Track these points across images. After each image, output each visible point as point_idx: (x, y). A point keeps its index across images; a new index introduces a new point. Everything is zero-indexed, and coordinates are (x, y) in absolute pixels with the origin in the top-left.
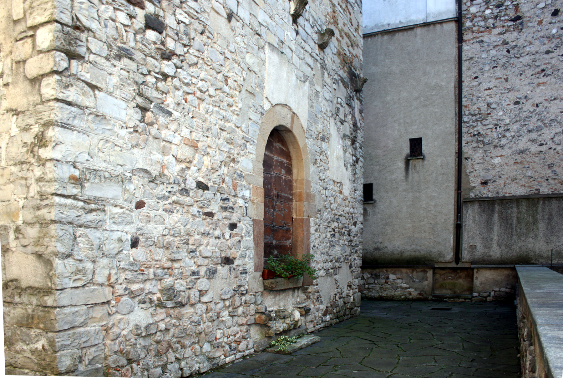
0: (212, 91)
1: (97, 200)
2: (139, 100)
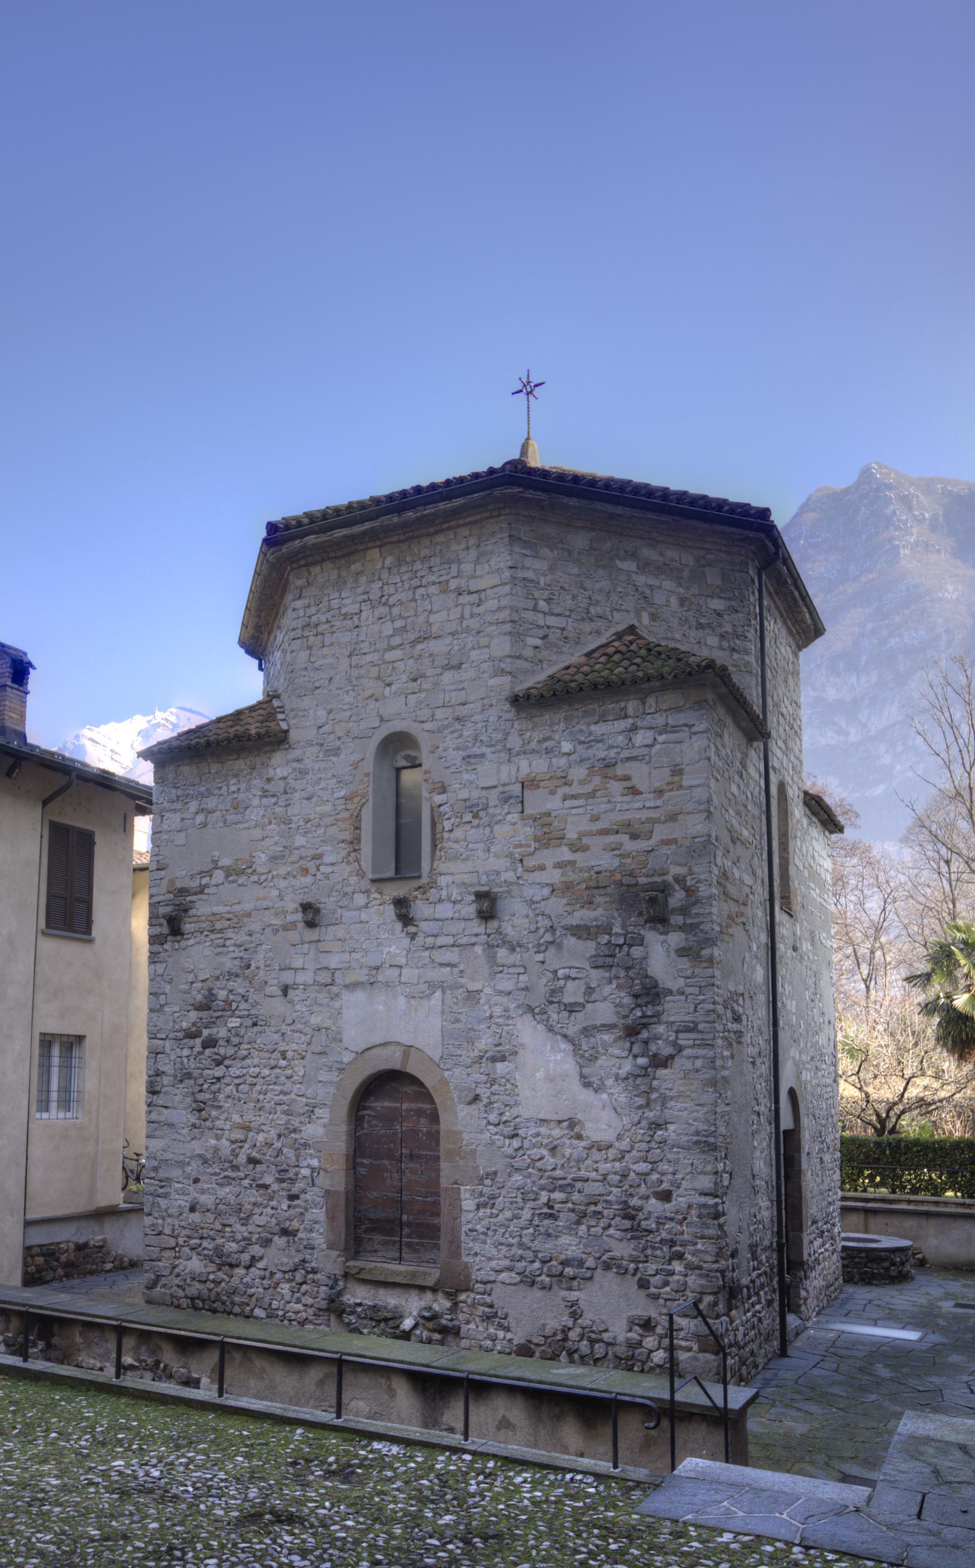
0: (266, 1072)
2: (194, 1105)
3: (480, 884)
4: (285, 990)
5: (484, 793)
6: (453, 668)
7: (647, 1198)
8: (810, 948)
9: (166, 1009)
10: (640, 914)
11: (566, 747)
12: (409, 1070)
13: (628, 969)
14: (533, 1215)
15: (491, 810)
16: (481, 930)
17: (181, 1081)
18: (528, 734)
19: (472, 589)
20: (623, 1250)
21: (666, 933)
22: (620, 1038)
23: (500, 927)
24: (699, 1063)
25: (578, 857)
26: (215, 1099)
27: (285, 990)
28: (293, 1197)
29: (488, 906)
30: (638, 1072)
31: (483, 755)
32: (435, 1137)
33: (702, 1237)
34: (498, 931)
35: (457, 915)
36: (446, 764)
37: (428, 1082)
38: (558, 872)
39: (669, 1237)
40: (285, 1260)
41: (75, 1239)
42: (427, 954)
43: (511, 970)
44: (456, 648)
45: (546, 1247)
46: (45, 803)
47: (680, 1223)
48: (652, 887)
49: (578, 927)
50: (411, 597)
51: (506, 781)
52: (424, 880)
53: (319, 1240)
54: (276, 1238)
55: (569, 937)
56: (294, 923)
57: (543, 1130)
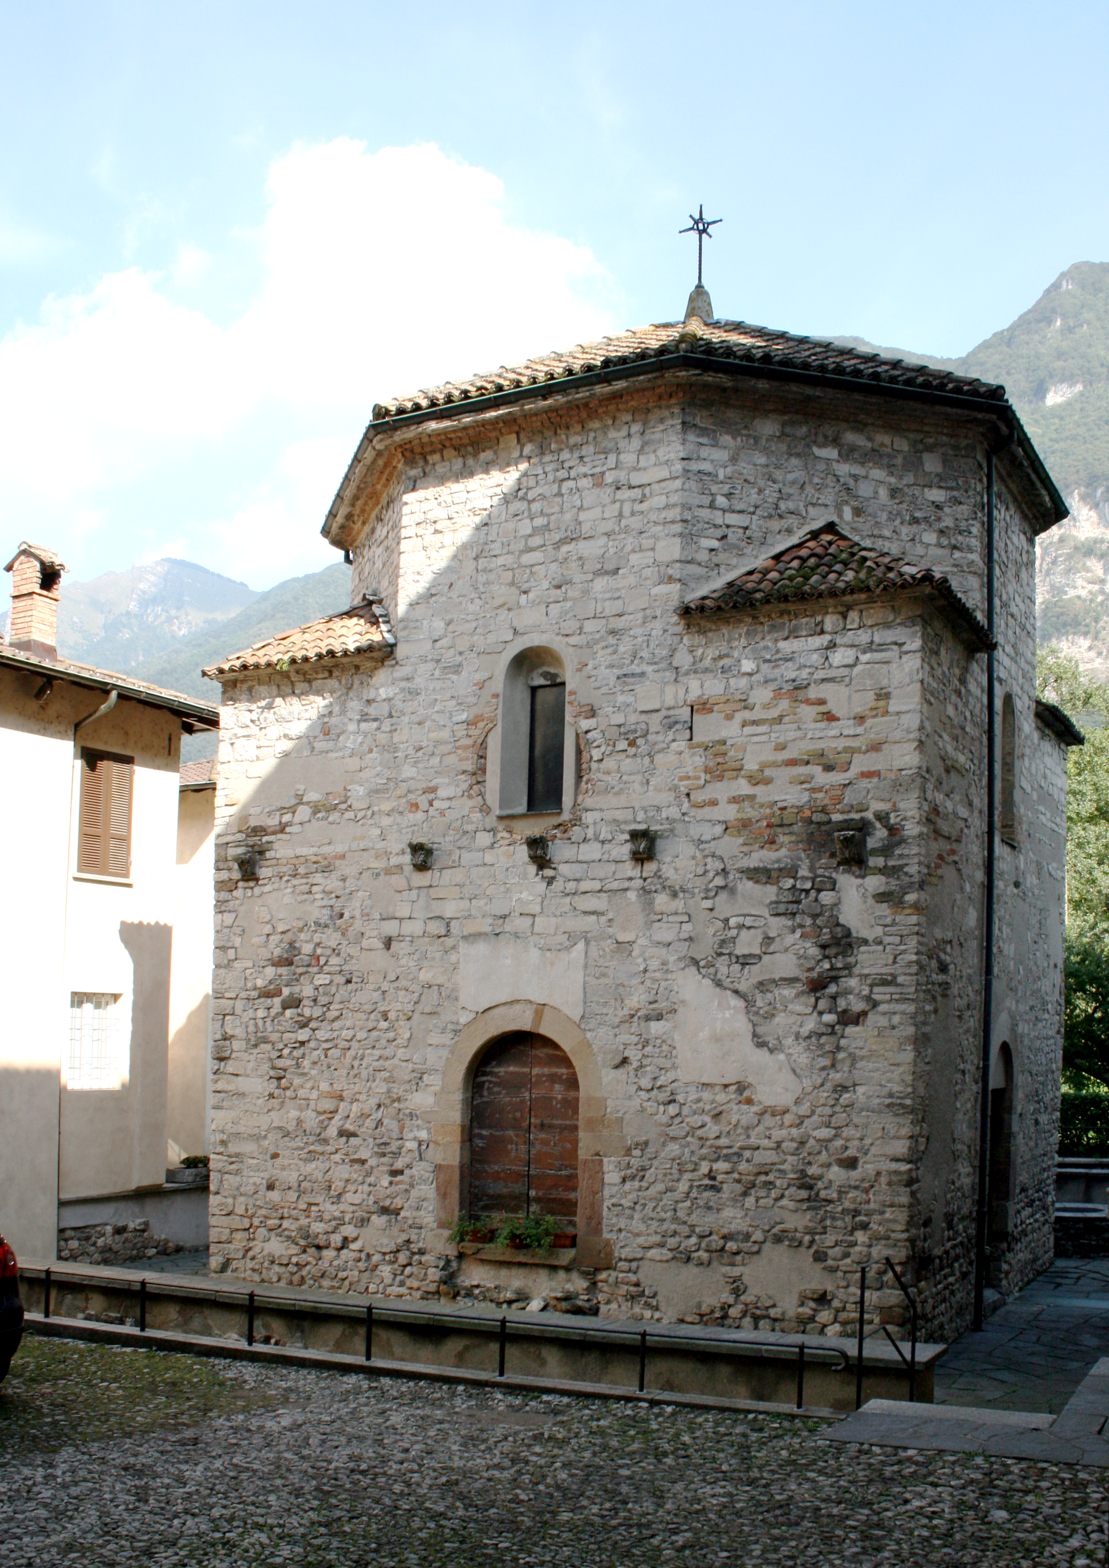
1: (237, 1155)
2: (272, 1073)
3: (635, 821)
4: (388, 943)
5: (644, 717)
6: (607, 573)
7: (829, 1165)
8: (1035, 881)
9: (236, 964)
10: (833, 855)
11: (748, 666)
12: (544, 1031)
13: (815, 916)
14: (691, 1187)
15: (649, 737)
16: (636, 873)
17: (256, 1046)
18: (700, 651)
19: (633, 483)
20: (798, 1221)
21: (863, 877)
22: (803, 993)
23: (659, 870)
24: (896, 1019)
25: (759, 790)
26: (298, 1066)
27: (388, 943)
28: (395, 1173)
29: (645, 845)
30: (824, 1030)
31: (643, 674)
32: (572, 1105)
33: (891, 1206)
34: (657, 875)
35: (606, 857)
36: (597, 684)
37: (566, 1045)
38: (735, 807)
39: (852, 1206)
40: (385, 1241)
41: (113, 1221)
42: (568, 900)
43: (671, 918)
44: (612, 551)
45: (704, 1221)
46: (77, 726)
47: (866, 1191)
48: (846, 825)
49: (756, 870)
50: (555, 491)
51: (672, 703)
52: (566, 816)
53: (428, 1218)
54: (374, 1217)
55: (745, 880)
56: (400, 867)
57: (706, 1095)
